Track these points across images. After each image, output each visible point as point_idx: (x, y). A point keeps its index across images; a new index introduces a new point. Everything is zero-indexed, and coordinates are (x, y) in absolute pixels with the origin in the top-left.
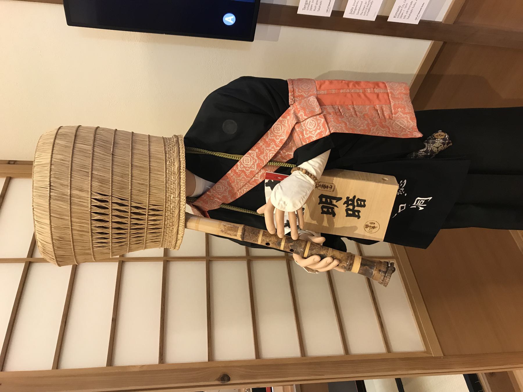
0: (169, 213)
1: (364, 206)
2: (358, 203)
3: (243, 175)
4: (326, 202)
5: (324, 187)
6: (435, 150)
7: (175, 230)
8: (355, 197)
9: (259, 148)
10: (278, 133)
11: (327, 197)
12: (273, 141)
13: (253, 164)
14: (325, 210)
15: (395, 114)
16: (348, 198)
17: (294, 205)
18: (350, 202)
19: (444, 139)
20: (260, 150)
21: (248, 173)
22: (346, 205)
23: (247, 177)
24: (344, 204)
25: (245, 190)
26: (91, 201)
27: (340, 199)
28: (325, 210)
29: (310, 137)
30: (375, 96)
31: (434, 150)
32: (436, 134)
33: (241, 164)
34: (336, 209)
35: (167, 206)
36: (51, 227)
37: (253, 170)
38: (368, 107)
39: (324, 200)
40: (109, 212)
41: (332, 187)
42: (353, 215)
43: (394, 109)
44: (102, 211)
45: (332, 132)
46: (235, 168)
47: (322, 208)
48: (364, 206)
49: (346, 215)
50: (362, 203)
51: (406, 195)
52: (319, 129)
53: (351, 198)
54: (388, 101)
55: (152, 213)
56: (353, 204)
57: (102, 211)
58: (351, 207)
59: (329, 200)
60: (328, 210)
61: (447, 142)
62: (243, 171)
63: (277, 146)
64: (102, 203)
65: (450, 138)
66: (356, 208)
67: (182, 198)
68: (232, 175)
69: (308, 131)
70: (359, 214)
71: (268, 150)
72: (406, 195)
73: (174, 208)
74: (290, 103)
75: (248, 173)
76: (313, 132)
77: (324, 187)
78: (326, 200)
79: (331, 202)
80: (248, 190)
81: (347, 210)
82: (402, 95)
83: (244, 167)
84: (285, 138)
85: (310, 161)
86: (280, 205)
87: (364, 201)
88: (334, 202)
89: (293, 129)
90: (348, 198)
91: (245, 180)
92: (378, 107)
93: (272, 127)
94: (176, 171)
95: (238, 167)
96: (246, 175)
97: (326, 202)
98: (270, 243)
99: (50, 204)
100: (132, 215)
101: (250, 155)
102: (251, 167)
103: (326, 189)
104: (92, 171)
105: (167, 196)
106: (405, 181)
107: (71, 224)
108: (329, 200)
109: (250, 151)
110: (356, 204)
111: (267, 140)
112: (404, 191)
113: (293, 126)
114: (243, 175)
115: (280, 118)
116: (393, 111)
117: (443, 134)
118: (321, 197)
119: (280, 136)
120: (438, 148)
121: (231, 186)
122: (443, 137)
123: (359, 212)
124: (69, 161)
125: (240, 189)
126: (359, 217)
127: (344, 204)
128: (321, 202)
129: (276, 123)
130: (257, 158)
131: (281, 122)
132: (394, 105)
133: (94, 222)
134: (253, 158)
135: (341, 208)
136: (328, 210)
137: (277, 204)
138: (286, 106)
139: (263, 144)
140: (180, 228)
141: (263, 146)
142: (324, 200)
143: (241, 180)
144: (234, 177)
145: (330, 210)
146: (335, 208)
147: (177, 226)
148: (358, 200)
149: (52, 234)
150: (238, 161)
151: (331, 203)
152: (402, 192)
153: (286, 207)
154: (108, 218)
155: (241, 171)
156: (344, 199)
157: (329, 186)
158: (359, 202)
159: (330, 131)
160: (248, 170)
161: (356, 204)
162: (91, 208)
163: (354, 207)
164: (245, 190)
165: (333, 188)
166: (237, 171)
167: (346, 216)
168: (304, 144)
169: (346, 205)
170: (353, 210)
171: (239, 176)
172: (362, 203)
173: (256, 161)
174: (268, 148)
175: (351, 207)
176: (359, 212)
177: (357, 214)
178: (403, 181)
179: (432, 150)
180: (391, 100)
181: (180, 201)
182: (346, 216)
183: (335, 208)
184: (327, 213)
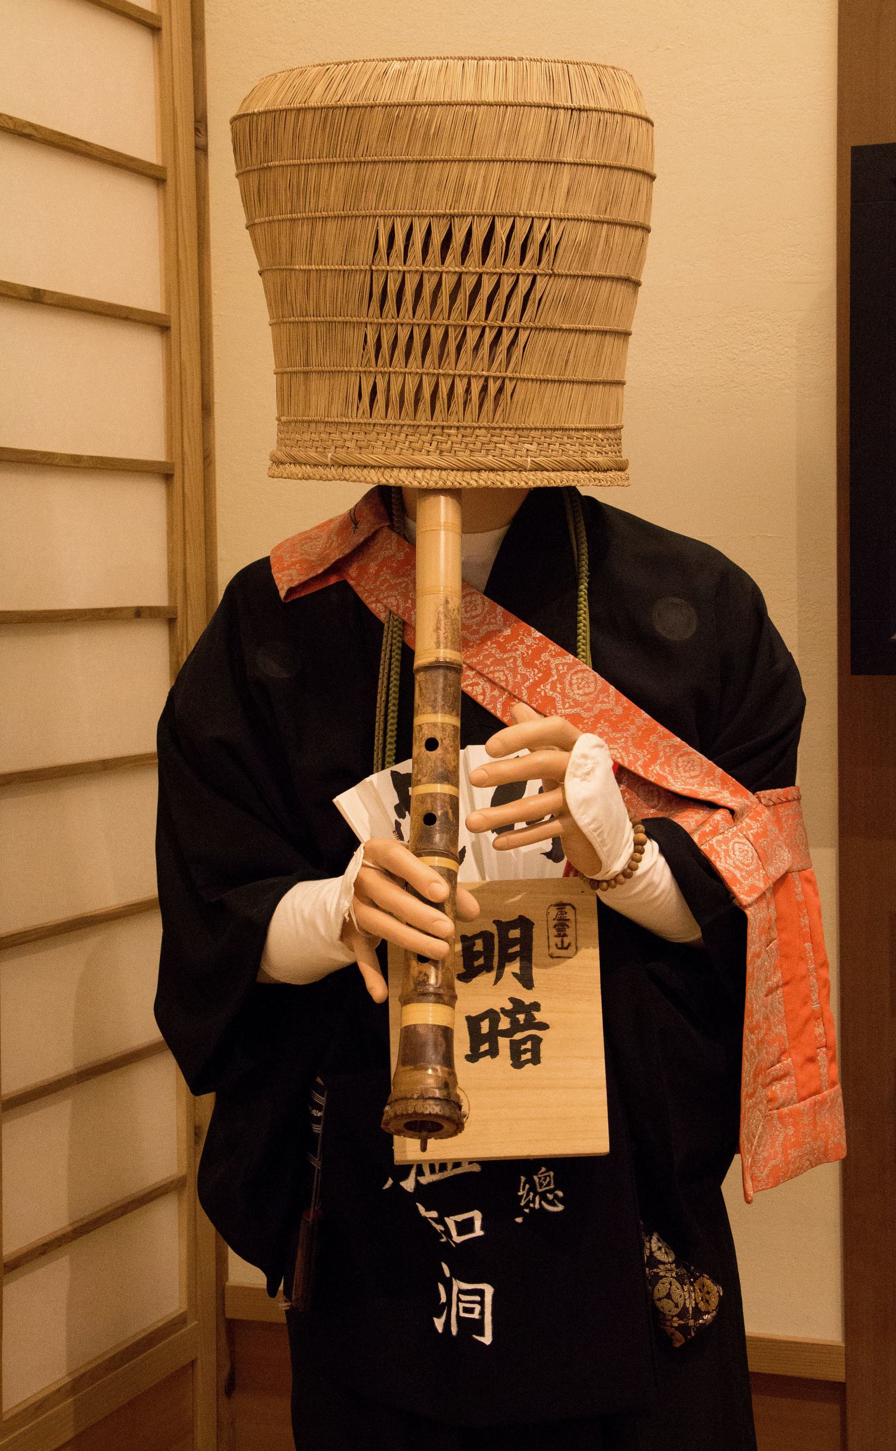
0: (486, 440)
1: (517, 1063)
2: (524, 1041)
3: (533, 675)
4: (506, 943)
5: (561, 926)
6: (661, 1289)
7: (422, 458)
8: (544, 1026)
9: (625, 716)
10: (677, 767)
11: (526, 942)
12: (654, 758)
13: (577, 704)
14: (479, 946)
15: (781, 1118)
16: (536, 1006)
17: (586, 802)
18: (521, 1017)
19: (698, 1312)
20: (621, 718)
21: (546, 689)
22: (509, 1006)
23: (532, 689)
24: (512, 1000)
25: (479, 689)
26: (545, 218)
27: (527, 981)
28: (479, 946)
29: (718, 853)
30: (809, 1053)
31: (659, 1286)
32: (709, 1282)
33: (570, 666)
34: (485, 979)
35: (505, 432)
36: (473, 104)
37: (559, 705)
38: (784, 1032)
39: (515, 933)
40: (512, 266)
41: (565, 948)
42: (476, 1038)
43: (790, 1114)
44: (516, 244)
45: (749, 912)
46: (554, 647)
47: (486, 936)
48: (517, 1063)
49: (473, 1015)
50: (527, 1054)
51: (519, 1220)
52: (742, 876)
53: (539, 1017)
54: (804, 1093)
55: (493, 388)
56: (516, 1027)
57: (516, 244)
58: (504, 1024)
59: (517, 948)
60: (478, 955)
61: (691, 1322)
62: (547, 674)
63: (645, 766)
64: (535, 246)
65: (703, 1330)
66: (504, 1043)
67: (531, 475)
68: (529, 641)
69: (727, 844)
70: (485, 1054)
71: (626, 742)
72: (519, 1220)
73: (498, 452)
74: (761, 793)
75: (546, 689)
76: (730, 861)
77: (561, 926)
78: (514, 942)
79: (511, 958)
80: (480, 699)
81: (492, 1015)
82: (823, 1135)
83: (561, 677)
84: (677, 786)
85: (662, 860)
86: (582, 761)
87: (536, 1059)
88: (514, 967)
89: (713, 806)
90: (536, 1006)
91: (517, 685)
92: (787, 1061)
93: (691, 749)
94: (590, 458)
95: (555, 657)
96: (536, 684)
97: (506, 943)
98: (439, 751)
99: (539, 106)
100: (495, 332)
101: (602, 691)
102: (564, 695)
103: (554, 932)
104: (609, 223)
105: (533, 433)
106: (560, 1208)
107: (481, 161)
108: (517, 948)
109: (612, 689)
110: (518, 1036)
111: (653, 738)
112: (532, 1210)
113: (722, 803)
114: (533, 675)
115: (719, 771)
116: (785, 1110)
117: (714, 1301)
118: (524, 924)
119: (671, 773)
120: (669, 1296)
121: (483, 640)
122: (702, 1305)
123: (493, 1052)
124: (615, 158)
125: (480, 674)
126: (474, 1057)
127: (512, 1000)
128: (503, 927)
129: (704, 759)
130: (596, 711)
131: (710, 773)
132: (799, 1113)
133: (485, 224)
134: (595, 701)
135: (487, 994)
136: (478, 955)
137: (586, 751)
138: (753, 784)
139: (639, 728)
140: (436, 473)
141: (633, 729)
142: (515, 933)
143: (514, 671)
144: (522, 648)
145: (481, 961)
146: (493, 975)
147: (443, 464)
148: (537, 1041)
149: (449, 104)
150: (576, 655)
151: (506, 959)
152: (527, 1206)
153: (577, 780)
154: (452, 264)
155: (548, 668)
156: (527, 997)
157: (566, 941)
158: (529, 1045)
159: (750, 905)
160: (553, 688)
161: (518, 1036)
162: (526, 217)
163: (506, 1033)
164: (479, 689)
165: (563, 953)
166: (545, 656)
167: (468, 1018)
168: (696, 838)
169: (509, 1006)
170: (494, 1034)
171: (529, 664)
172: (527, 1054)
173: (588, 710)
174: (630, 743)
175: (504, 1024)
176: (493, 1052)
177: (485, 1047)
178: (561, 1201)
179: (657, 1278)
180: (809, 1101)
181: (521, 468)
182: (468, 1018)
183: (493, 975)
184: (468, 954)
